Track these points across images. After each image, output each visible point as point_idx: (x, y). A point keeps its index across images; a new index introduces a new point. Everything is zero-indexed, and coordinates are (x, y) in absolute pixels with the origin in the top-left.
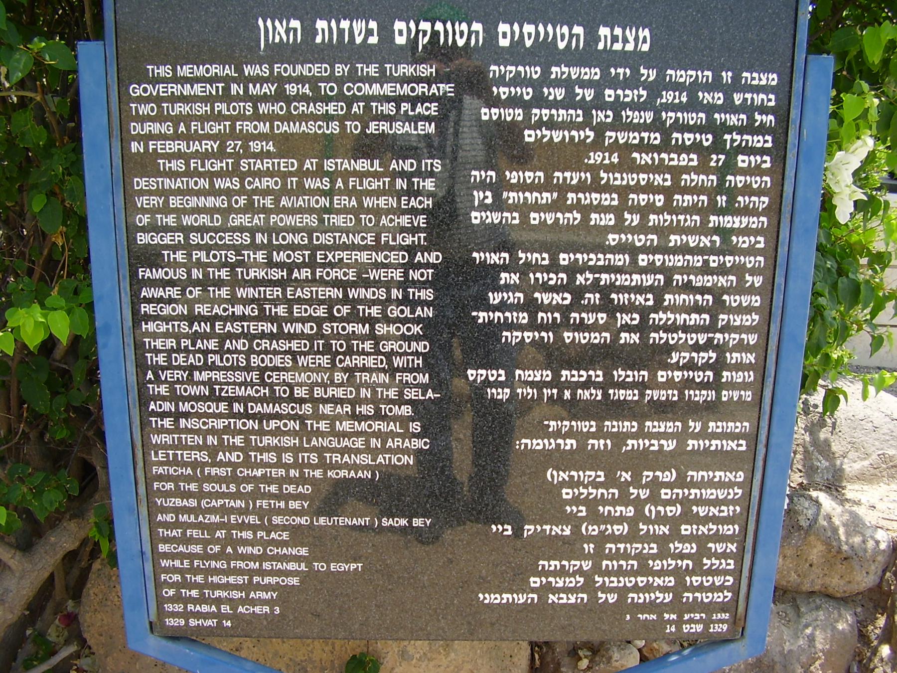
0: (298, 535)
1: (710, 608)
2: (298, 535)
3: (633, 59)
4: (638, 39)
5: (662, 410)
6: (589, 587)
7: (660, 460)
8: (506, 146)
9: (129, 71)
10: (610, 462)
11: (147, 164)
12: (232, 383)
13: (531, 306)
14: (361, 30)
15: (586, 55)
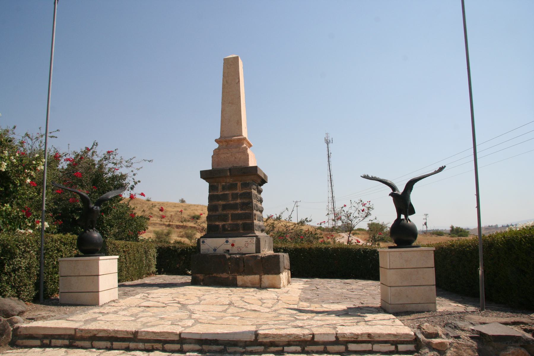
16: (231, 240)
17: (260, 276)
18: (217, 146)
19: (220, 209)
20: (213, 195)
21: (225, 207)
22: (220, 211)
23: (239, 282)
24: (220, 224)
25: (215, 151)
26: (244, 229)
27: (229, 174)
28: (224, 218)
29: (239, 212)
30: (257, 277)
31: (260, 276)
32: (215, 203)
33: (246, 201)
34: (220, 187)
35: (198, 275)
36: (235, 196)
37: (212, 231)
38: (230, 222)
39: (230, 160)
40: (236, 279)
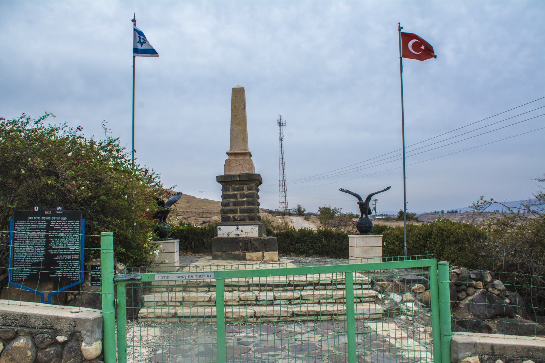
1: (77, 277)
3: (65, 220)
4: (65, 218)
5: (69, 254)
6: (62, 274)
7: (69, 260)
8: (53, 229)
10: (64, 260)
13: (55, 244)
15: (60, 220)
16: (240, 227)
17: (263, 253)
19: (231, 204)
20: (226, 194)
21: (235, 204)
22: (231, 207)
23: (248, 258)
24: (232, 215)
25: (227, 161)
27: (238, 179)
28: (234, 211)
30: (261, 253)
31: (263, 253)
35: (217, 253)
36: (242, 196)
37: (226, 221)
40: (245, 255)
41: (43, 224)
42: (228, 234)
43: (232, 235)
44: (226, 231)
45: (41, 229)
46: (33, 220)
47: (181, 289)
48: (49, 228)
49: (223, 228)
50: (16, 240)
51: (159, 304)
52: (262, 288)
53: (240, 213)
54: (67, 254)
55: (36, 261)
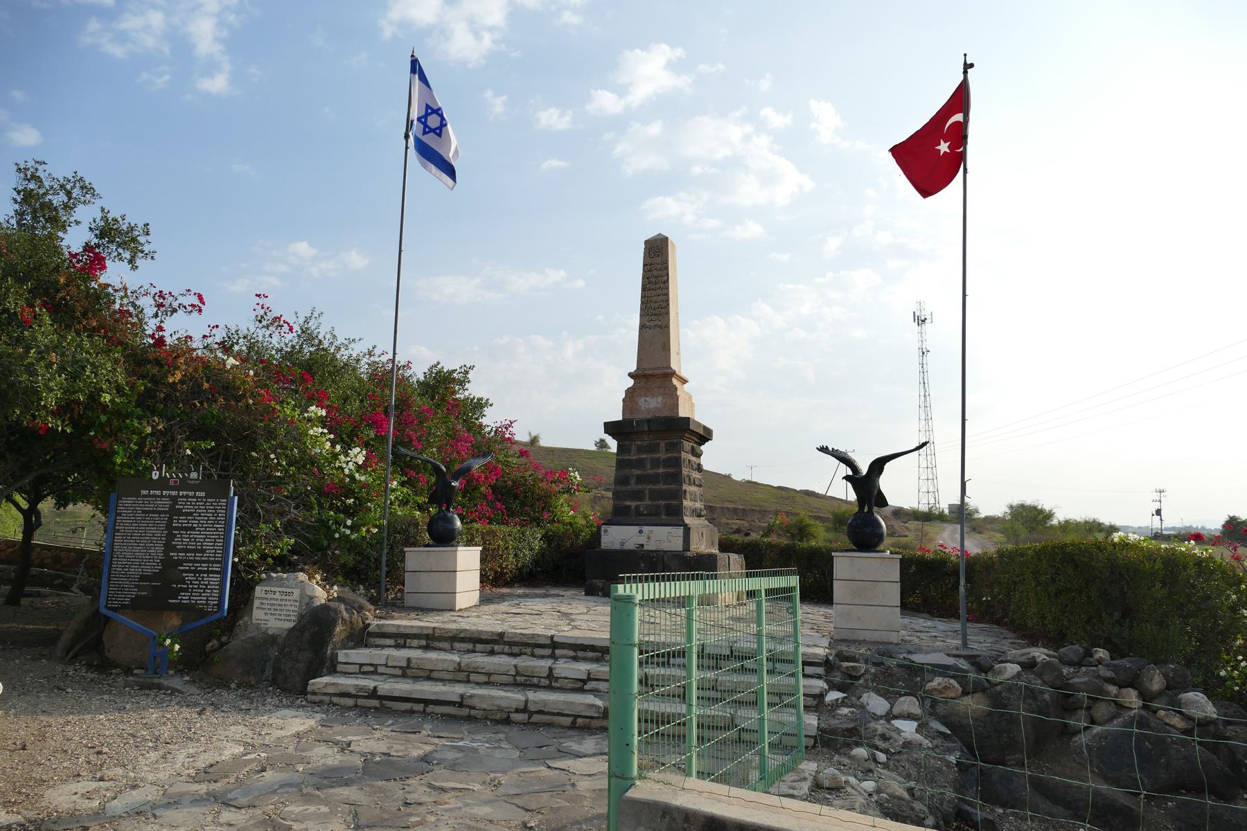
0: (136, 586)
2: (136, 586)
4: (203, 494)
5: (205, 562)
7: (204, 572)
9: (119, 498)
10: (195, 572)
11: (120, 514)
12: (129, 555)
14: (158, 492)
16: (646, 529)
18: (631, 382)
19: (633, 481)
21: (640, 479)
22: (633, 486)
24: (633, 504)
25: (629, 392)
26: (668, 514)
27: (646, 428)
28: (637, 495)
29: (661, 486)
32: (626, 472)
33: (671, 470)
34: (634, 448)
36: (656, 463)
37: (620, 516)
38: (647, 502)
39: (651, 404)
41: (164, 504)
42: (622, 544)
43: (631, 545)
44: (617, 537)
45: (160, 512)
46: (148, 496)
47: (423, 643)
48: (174, 512)
49: (614, 530)
50: (118, 531)
51: (366, 669)
52: (580, 654)
53: (650, 499)
54: (201, 562)
55: (148, 571)
